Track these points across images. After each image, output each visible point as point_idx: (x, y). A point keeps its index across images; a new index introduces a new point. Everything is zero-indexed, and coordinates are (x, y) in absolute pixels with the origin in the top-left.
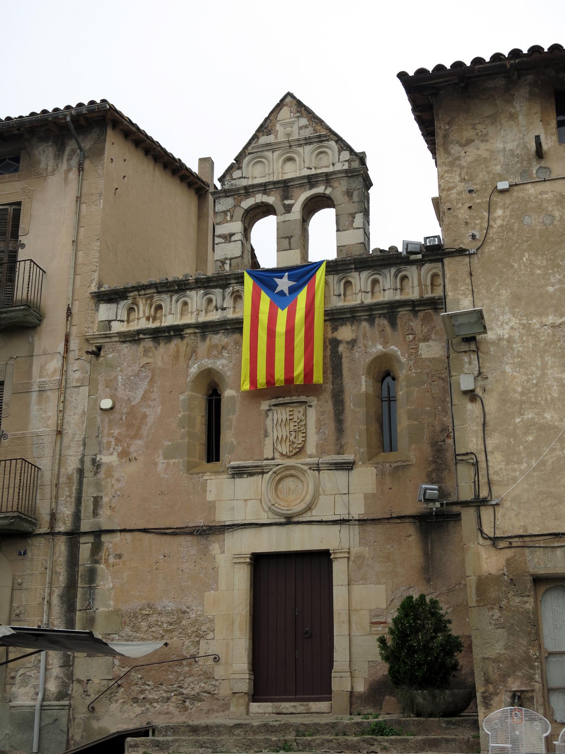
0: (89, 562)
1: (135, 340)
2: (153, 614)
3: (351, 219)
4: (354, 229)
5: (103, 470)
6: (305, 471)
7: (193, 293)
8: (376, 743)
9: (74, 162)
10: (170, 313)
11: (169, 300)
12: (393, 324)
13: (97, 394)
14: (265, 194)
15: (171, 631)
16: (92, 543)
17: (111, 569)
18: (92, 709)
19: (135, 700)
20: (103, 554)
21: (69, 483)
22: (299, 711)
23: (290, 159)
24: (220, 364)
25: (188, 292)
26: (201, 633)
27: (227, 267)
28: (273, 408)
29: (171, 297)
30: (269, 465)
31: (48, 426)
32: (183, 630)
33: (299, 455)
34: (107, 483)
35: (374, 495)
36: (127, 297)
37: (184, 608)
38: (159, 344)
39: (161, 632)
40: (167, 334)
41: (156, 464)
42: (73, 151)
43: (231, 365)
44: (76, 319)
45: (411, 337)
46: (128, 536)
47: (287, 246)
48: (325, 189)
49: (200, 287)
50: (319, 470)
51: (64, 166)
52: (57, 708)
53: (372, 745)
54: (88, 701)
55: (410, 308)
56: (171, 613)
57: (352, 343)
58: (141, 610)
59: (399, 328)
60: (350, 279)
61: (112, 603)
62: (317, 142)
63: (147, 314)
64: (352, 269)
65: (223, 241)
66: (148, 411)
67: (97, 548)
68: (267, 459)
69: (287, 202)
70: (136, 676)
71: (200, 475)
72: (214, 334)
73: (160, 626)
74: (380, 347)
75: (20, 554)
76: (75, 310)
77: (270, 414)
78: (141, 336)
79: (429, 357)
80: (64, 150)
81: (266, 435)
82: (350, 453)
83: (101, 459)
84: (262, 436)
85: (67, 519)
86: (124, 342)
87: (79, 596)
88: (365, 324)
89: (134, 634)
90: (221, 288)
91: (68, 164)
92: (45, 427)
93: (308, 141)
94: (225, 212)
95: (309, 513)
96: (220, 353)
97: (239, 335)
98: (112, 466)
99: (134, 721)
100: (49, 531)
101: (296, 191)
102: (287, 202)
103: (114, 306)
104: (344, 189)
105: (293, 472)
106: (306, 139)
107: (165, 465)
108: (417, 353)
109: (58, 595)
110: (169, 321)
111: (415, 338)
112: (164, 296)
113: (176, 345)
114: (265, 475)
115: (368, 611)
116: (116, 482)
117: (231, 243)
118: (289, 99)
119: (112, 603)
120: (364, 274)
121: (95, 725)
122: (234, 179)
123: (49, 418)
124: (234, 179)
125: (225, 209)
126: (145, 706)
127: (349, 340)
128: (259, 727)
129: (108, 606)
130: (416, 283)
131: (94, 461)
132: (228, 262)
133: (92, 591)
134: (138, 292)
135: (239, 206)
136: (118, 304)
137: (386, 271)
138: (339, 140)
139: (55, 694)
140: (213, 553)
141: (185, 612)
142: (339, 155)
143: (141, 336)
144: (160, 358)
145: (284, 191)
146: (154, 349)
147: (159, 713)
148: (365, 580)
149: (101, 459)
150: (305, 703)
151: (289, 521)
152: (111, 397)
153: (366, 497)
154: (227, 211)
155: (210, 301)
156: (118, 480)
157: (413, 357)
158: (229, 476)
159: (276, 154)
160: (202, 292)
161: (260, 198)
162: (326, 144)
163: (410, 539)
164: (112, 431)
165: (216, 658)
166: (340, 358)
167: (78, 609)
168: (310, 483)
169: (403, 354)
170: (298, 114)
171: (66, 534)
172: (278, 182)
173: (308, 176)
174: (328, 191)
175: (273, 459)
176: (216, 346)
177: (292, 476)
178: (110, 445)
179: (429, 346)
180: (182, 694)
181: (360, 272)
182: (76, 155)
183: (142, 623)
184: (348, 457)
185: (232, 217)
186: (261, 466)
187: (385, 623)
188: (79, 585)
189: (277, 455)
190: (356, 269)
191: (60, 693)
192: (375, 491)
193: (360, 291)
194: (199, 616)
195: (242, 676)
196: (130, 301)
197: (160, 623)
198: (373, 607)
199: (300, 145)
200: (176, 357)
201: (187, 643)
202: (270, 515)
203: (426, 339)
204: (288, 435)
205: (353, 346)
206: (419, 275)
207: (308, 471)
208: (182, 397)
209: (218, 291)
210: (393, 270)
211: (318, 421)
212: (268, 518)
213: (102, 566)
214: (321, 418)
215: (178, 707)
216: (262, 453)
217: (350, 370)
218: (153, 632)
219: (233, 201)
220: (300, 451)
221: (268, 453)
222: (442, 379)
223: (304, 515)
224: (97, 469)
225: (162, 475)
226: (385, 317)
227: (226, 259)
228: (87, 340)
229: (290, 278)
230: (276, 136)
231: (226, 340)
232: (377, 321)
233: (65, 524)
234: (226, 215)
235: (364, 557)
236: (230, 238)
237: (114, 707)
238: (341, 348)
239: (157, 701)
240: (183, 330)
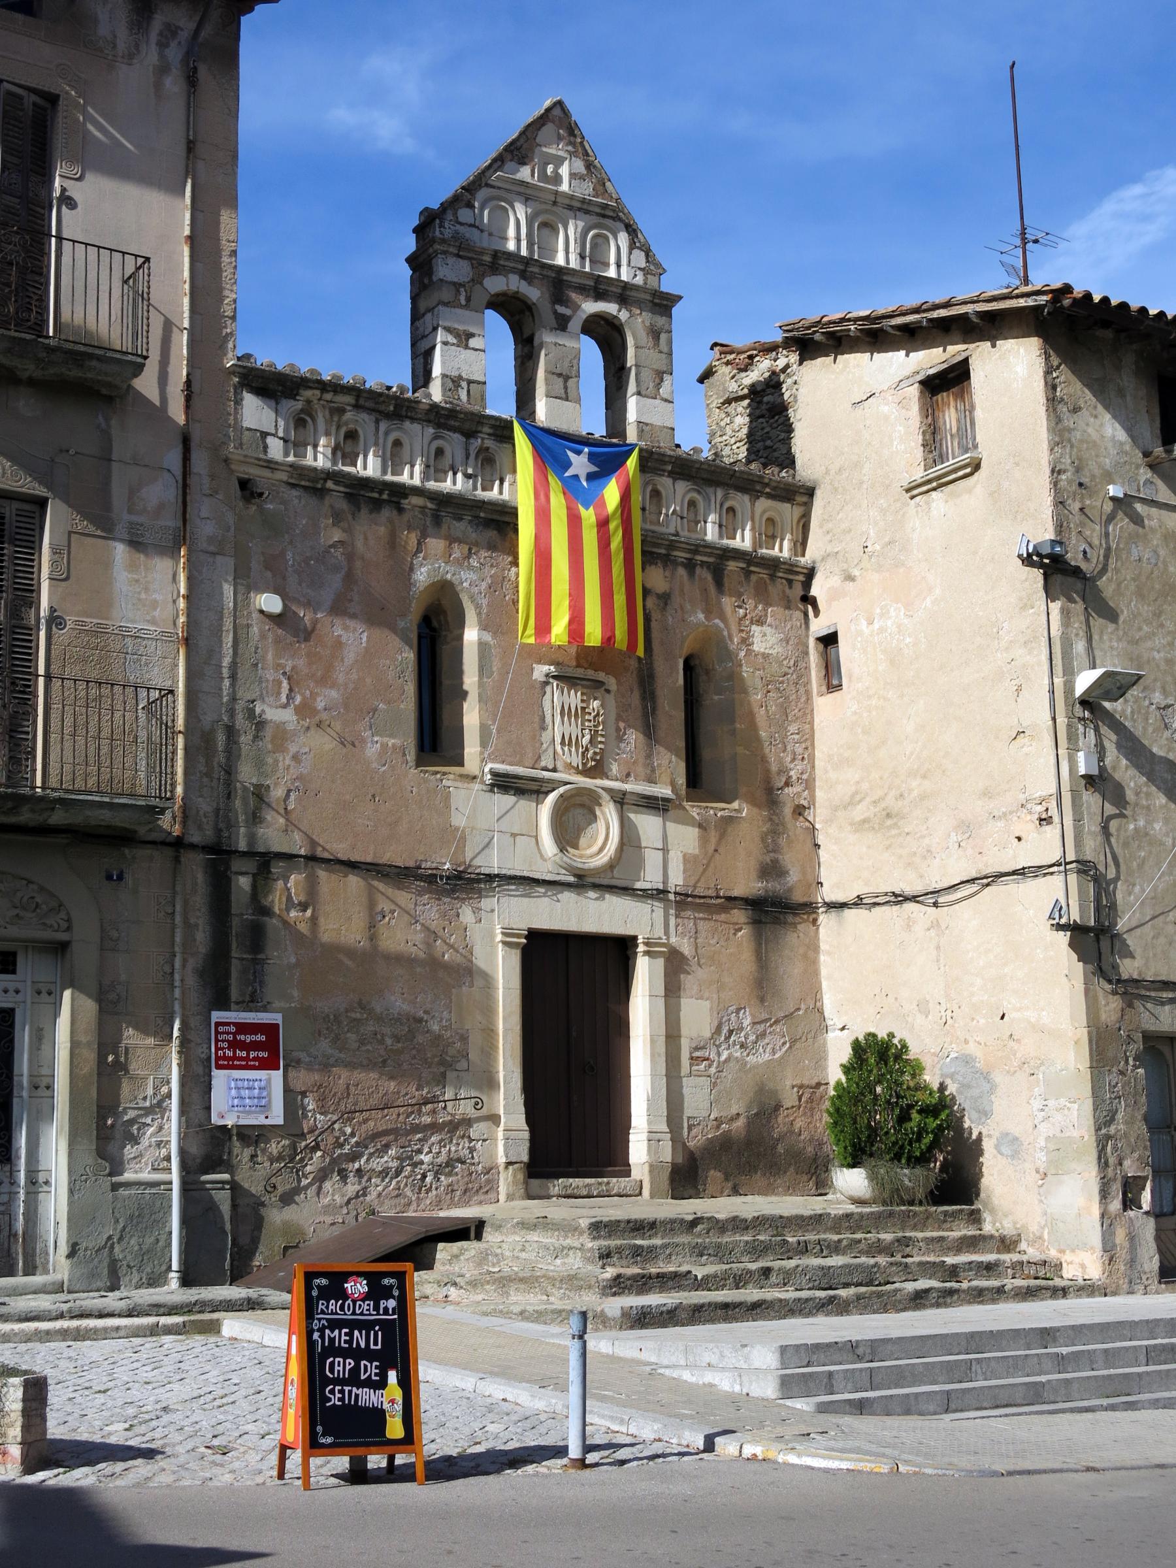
0: (250, 911)
2: (367, 1019)
3: (657, 380)
5: (268, 732)
7: (416, 428)
9: (174, 53)
13: (249, 577)
27: (463, 395)
29: (377, 422)
31: (153, 622)
32: (418, 1051)
34: (276, 761)
35: (695, 857)
37: (421, 1014)
40: (376, 495)
42: (171, 31)
43: (484, 585)
48: (619, 311)
49: (429, 421)
51: (151, 55)
55: (744, 565)
56: (398, 1020)
57: (665, 598)
61: (296, 993)
62: (598, 214)
64: (664, 471)
65: (455, 341)
66: (346, 637)
68: (545, 769)
69: (561, 309)
72: (455, 519)
74: (701, 616)
75: (109, 877)
79: (762, 650)
80: (149, 19)
84: (536, 726)
85: (204, 820)
86: (293, 486)
87: (234, 974)
90: (463, 434)
91: (162, 56)
92: (148, 621)
93: (585, 207)
94: (457, 286)
98: (285, 731)
102: (561, 309)
106: (583, 201)
112: (364, 416)
113: (391, 521)
116: (293, 763)
117: (468, 351)
118: (557, 112)
119: (296, 993)
120: (682, 486)
122: (461, 224)
123: (154, 605)
124: (461, 224)
125: (456, 280)
131: (251, 713)
133: (258, 967)
134: (322, 393)
135: (481, 284)
136: (277, 403)
137: (710, 490)
139: (198, 1161)
141: (420, 1020)
142: (630, 253)
143: (330, 484)
144: (361, 537)
146: (350, 517)
149: (263, 711)
154: (460, 285)
156: (296, 758)
158: (485, 788)
161: (513, 283)
164: (282, 661)
165: (477, 1104)
167: (233, 999)
170: (570, 148)
171: (206, 849)
174: (624, 315)
175: (554, 770)
178: (280, 687)
181: (675, 480)
182: (176, 42)
183: (349, 1035)
185: (468, 299)
188: (234, 954)
192: (697, 851)
194: (446, 1028)
205: (666, 604)
210: (720, 493)
219: (469, 268)
224: (258, 730)
226: (708, 568)
227: (460, 377)
229: (592, 457)
231: (474, 535)
234: (458, 291)
236: (467, 340)
240: (405, 496)
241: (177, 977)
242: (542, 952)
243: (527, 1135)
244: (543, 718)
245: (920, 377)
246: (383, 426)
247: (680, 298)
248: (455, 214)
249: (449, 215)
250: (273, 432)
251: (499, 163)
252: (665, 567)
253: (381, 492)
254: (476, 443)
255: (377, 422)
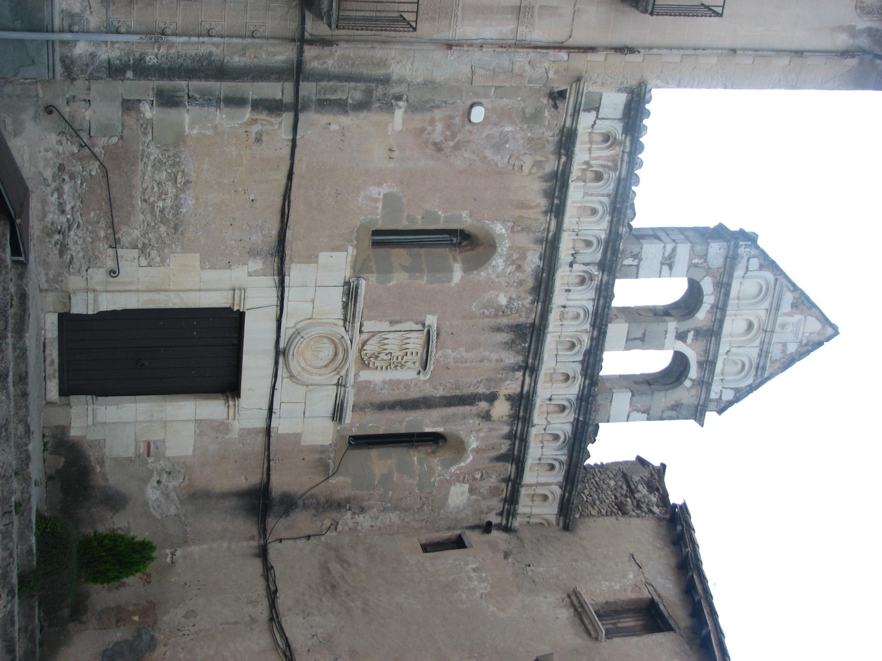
0: (255, 97)
1: (560, 148)
2: (177, 187)
3: (643, 409)
4: (629, 413)
6: (338, 373)
7: (605, 225)
8: (10, 598)
10: (586, 194)
11: (605, 192)
12: (500, 458)
14: (712, 308)
15: (152, 211)
16: (281, 101)
17: (243, 130)
18: (49, 110)
19: (61, 168)
20: (263, 116)
21: (373, 64)
22: (48, 368)
23: (750, 326)
24: (498, 262)
25: (608, 218)
26: (148, 250)
27: (628, 261)
28: (426, 330)
30: (353, 330)
33: (361, 362)
35: (299, 442)
36: (626, 135)
38: (546, 181)
39: (152, 199)
40: (556, 194)
41: (379, 184)
43: (493, 277)
44: (616, 59)
45: (478, 476)
46: (287, 151)
47: (632, 336)
48: (691, 380)
49: (610, 234)
50: (338, 385)
52: (51, 62)
53: (8, 595)
54: (60, 103)
57: (487, 416)
58: (183, 171)
59: (492, 465)
60: (567, 411)
61: (195, 132)
63: (592, 162)
64: (579, 415)
65: (666, 255)
67: (273, 107)
70: (94, 168)
71: (355, 242)
72: (541, 255)
73: (160, 197)
74: (474, 445)
76: (630, 58)
77: (419, 327)
78: (563, 159)
81: (392, 323)
82: (352, 418)
83: (400, 107)
88: (506, 429)
89: (150, 164)
90: (601, 261)
93: (764, 354)
94: (705, 256)
95: (286, 374)
96: (513, 263)
97: (532, 286)
99: (33, 169)
100: (307, 36)
101: (701, 344)
103: (619, 114)
104: (683, 402)
105: (340, 356)
106: (767, 352)
107: (376, 196)
108: (458, 481)
109: (211, 54)
110: (575, 194)
111: (475, 479)
113: (538, 206)
114: (341, 323)
115: (162, 438)
119: (195, 132)
120: (568, 428)
121: (27, 116)
122: (748, 261)
124: (748, 261)
125: (709, 255)
126: (54, 181)
127: (492, 413)
128: (27, 451)
129: (192, 127)
130: (542, 480)
131: (399, 98)
132: (636, 262)
137: (565, 451)
138: (752, 388)
140: (250, 263)
142: (732, 389)
143: (563, 159)
145: (707, 331)
146: (540, 174)
147: (44, 202)
148: (199, 435)
150: (57, 375)
151: (280, 353)
152: (486, 117)
153: (298, 436)
154: (706, 259)
155: (588, 244)
157: (454, 478)
159: (763, 314)
160: (603, 236)
161: (709, 300)
162: (753, 372)
163: (243, 478)
165: (114, 273)
166: (471, 404)
168: (323, 377)
169: (460, 468)
170: (805, 341)
171: (300, 63)
172: (721, 327)
173: (715, 363)
174: (687, 383)
175: (361, 332)
176: (523, 257)
177: (336, 354)
179: (463, 493)
180: (69, 230)
181: (572, 423)
183: (165, 173)
184: (348, 416)
185: (696, 266)
186: (353, 322)
187: (148, 455)
189: (364, 336)
190: (577, 420)
191: (73, 61)
192: (303, 444)
193: (549, 423)
195: (91, 307)
196: (620, 137)
197: (163, 197)
198: (167, 444)
199: (762, 343)
200: (523, 205)
201: (136, 233)
202: (290, 332)
203: (472, 491)
204: (387, 351)
205: (483, 417)
206: (550, 484)
207: (338, 377)
208: (464, 214)
209: (598, 256)
210: (564, 458)
211: (398, 382)
212: (287, 328)
213: (248, 115)
214: (402, 386)
215: (52, 224)
216: (369, 319)
217: (454, 415)
218: (153, 188)
219: (717, 266)
220: (364, 363)
221: (369, 326)
222: (421, 508)
223: (285, 370)
225: (362, 194)
226: (509, 450)
227: (640, 260)
228: (579, 80)
230: (787, 314)
231: (529, 269)
232: (509, 442)
233: (316, 58)
235: (227, 433)
236: (667, 264)
237: (53, 137)
238: (483, 405)
239: (60, 196)
240: (557, 217)
241: (206, 39)
242: (229, 323)
243: (90, 312)
244: (399, 322)
245: (656, 598)
246: (606, 200)
247: (702, 425)
248: (754, 256)
249: (754, 252)
250: (600, 116)
251: (792, 289)
252: (510, 416)
253: (559, 198)
254: (594, 271)
255: (608, 195)
